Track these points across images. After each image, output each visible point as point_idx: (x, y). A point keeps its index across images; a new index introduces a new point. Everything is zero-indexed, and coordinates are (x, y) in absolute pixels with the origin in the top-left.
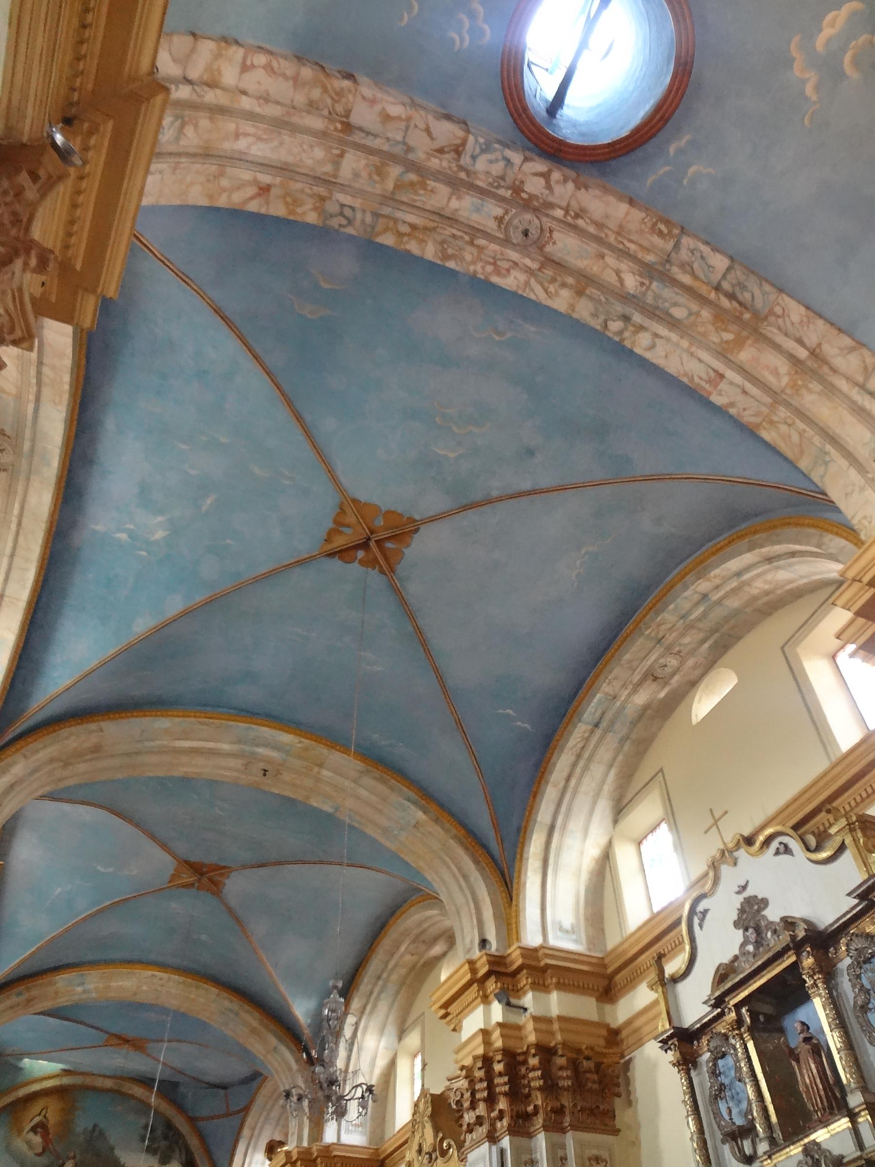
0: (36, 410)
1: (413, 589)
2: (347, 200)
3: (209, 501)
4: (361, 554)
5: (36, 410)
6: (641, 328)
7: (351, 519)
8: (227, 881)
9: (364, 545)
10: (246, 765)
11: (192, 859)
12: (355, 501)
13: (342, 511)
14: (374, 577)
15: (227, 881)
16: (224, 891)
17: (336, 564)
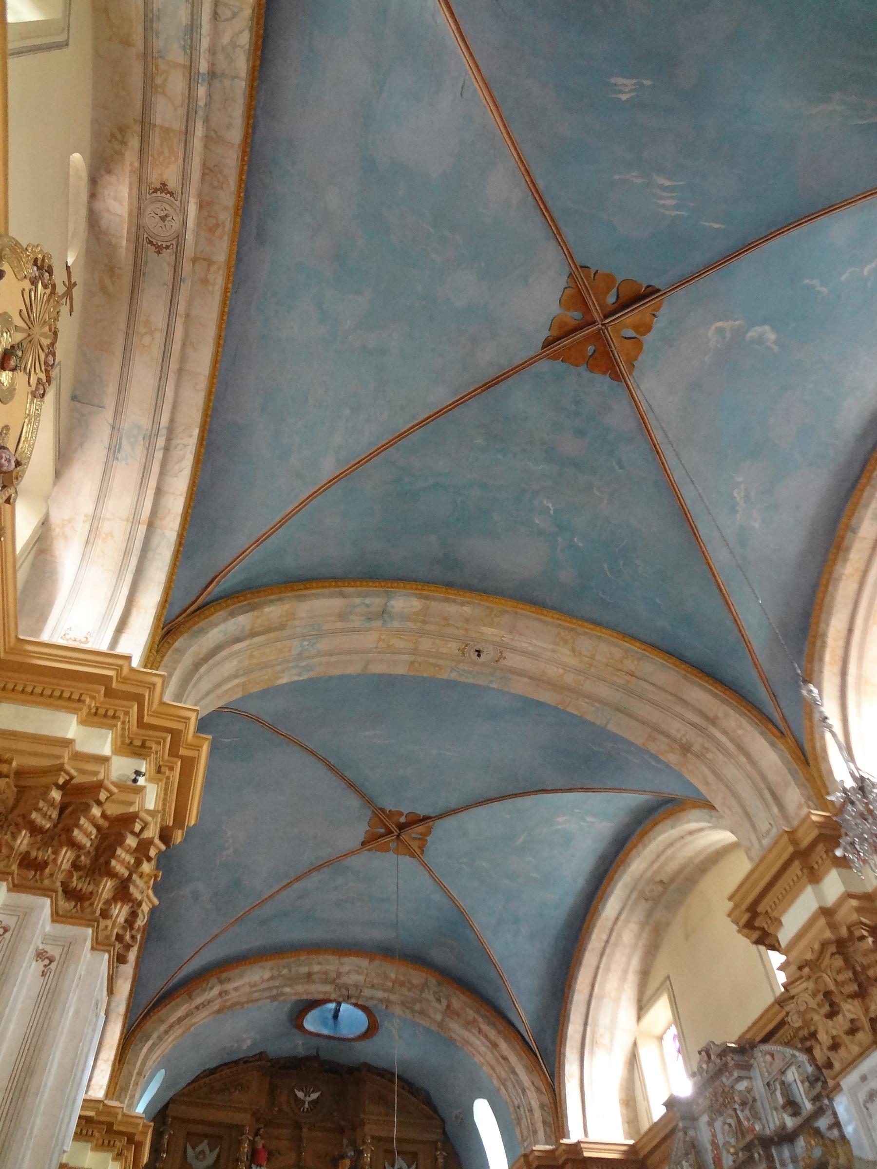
0: (620, 914)
1: (354, 802)
2: (437, 1005)
3: (521, 840)
4: (403, 820)
5: (620, 914)
6: (272, 978)
7: (414, 845)
9: (402, 827)
10: (501, 657)
12: (412, 856)
13: (421, 848)
14: (389, 804)
16: (563, 281)
17: (422, 811)
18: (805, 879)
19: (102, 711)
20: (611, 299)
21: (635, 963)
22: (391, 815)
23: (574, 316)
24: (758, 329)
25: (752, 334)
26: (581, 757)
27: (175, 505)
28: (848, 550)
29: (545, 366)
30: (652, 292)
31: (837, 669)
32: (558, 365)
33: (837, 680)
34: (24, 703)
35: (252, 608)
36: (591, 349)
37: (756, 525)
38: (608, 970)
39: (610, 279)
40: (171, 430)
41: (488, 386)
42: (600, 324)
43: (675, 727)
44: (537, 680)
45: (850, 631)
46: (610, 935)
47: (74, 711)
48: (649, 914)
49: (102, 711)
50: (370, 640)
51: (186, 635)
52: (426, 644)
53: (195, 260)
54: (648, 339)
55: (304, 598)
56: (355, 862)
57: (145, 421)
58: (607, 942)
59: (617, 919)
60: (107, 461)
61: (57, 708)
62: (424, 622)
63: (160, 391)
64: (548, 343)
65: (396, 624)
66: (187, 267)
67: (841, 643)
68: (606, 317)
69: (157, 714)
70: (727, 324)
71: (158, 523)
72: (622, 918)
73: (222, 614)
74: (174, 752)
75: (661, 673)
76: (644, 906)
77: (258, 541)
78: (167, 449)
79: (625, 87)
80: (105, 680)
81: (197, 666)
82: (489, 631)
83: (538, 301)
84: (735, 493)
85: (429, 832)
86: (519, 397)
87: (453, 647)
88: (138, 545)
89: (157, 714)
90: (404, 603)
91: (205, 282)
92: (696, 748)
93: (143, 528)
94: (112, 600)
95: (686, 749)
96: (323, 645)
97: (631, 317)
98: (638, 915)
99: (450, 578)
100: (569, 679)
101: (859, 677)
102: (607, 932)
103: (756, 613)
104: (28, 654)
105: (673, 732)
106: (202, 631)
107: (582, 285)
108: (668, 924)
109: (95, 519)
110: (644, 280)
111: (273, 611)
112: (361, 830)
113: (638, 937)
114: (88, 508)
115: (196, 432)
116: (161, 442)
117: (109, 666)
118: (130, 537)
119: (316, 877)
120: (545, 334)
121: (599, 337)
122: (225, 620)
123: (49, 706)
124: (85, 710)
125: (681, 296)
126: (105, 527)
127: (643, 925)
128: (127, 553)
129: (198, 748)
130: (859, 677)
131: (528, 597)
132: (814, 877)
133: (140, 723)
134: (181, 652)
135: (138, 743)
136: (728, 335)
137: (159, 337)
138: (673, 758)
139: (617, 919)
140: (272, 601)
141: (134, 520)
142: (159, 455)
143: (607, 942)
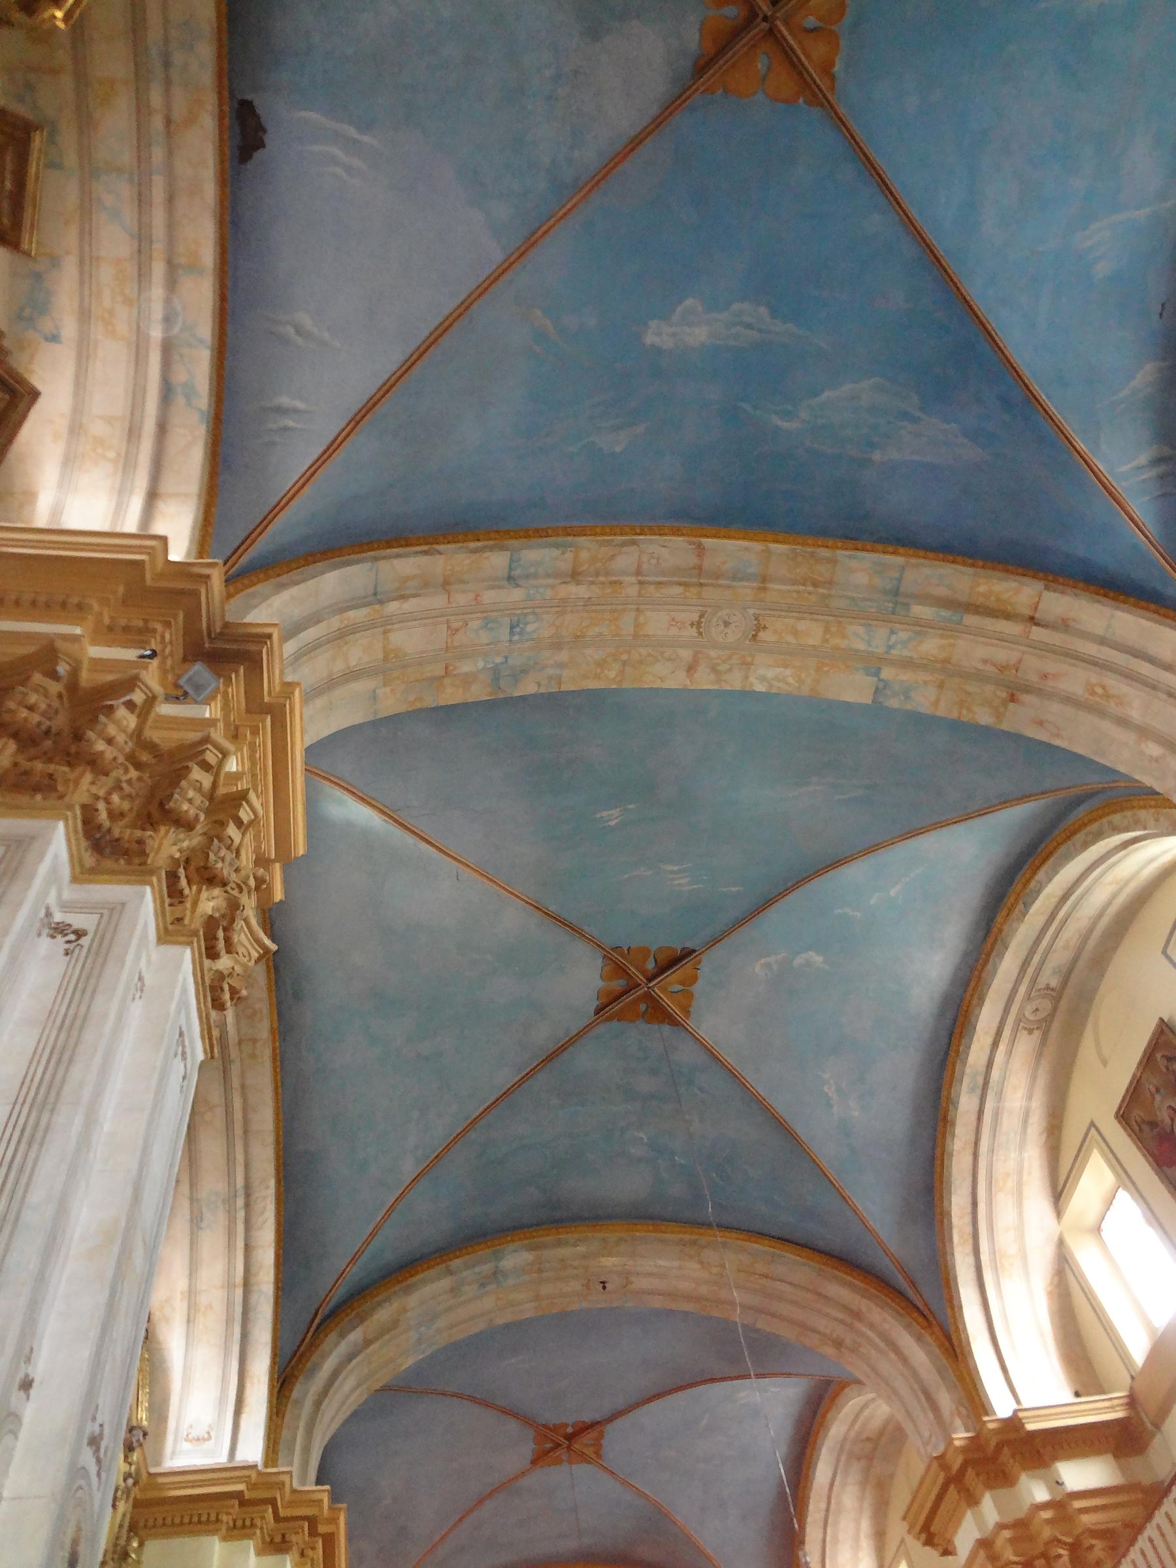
1: (512, 1425)
3: (705, 1422)
4: (570, 1430)
7: (589, 1451)
8: (600, 984)
9: (570, 1438)
10: (628, 1283)
11: (666, 1029)
13: (598, 1454)
14: (550, 1417)
15: (600, 984)
16: (599, 962)
17: (587, 1417)
18: (963, 1504)
19: (239, 1523)
20: (650, 965)
21: (866, 1525)
22: (555, 1429)
23: (619, 984)
24: (804, 956)
25: (798, 961)
26: (739, 1351)
27: (266, 1256)
28: (953, 1124)
29: (601, 1029)
30: (688, 953)
31: (969, 1248)
32: (615, 1025)
33: (971, 1260)
34: (166, 1536)
35: (362, 1319)
36: (643, 1007)
37: (856, 1114)
38: (836, 1541)
39: (645, 952)
40: (247, 1187)
41: (550, 1058)
42: (645, 986)
43: (821, 1324)
44: (671, 1295)
45: (975, 1204)
46: (829, 1503)
47: (213, 1532)
48: (867, 1471)
49: (239, 1523)
50: (488, 1303)
51: (301, 1378)
52: (547, 1289)
53: (240, 1043)
54: (697, 988)
55: (407, 1291)
56: (526, 1482)
57: (221, 1187)
58: (828, 1510)
59: (832, 1485)
60: (192, 1234)
61: (199, 1533)
62: (540, 1271)
63: (230, 1159)
64: (598, 1011)
65: (511, 1281)
66: (234, 1053)
67: (968, 1219)
68: (650, 980)
69: (291, 1504)
70: (771, 959)
71: (253, 1280)
72: (837, 1483)
73: (333, 1336)
74: (313, 1533)
75: (797, 1270)
76: (856, 1468)
77: (353, 1260)
78: (247, 1205)
79: (612, 816)
80: (238, 1495)
81: (318, 1404)
82: (609, 1262)
83: (583, 980)
84: (826, 1089)
85: (601, 1435)
86: (582, 1059)
87: (576, 1285)
88: (238, 1309)
89: (291, 1504)
90: (515, 1258)
91: (253, 1056)
92: (848, 1342)
93: (239, 1292)
94: (224, 1379)
95: (838, 1344)
96: (441, 1323)
97: (672, 979)
98: (855, 1475)
99: (556, 1219)
100: (703, 1290)
101: (993, 1252)
102: (825, 1500)
103: (876, 1205)
104: (161, 1487)
105: (822, 1329)
106: (317, 1367)
107: (617, 962)
108: (892, 1476)
109: (192, 1294)
110: (677, 944)
111: (382, 1315)
112: (527, 1449)
113: (861, 1499)
114: (182, 1284)
115: (272, 1183)
116: (240, 1202)
117: (238, 1480)
118: (230, 1304)
119: (489, 1505)
120: (594, 1004)
121: (649, 997)
122: (337, 1344)
123: (192, 1533)
124: (224, 1528)
125: (719, 951)
126: (203, 1300)
127: (863, 1483)
128: (229, 1321)
129: (334, 1521)
130: (993, 1252)
131: (645, 1217)
132: (972, 1500)
133: (277, 1518)
134: (299, 1403)
135: (278, 1539)
136: (775, 967)
137: (220, 1112)
138: (829, 1351)
139: (832, 1485)
140: (379, 1304)
141: (230, 1286)
142: (241, 1214)
143: (828, 1510)
